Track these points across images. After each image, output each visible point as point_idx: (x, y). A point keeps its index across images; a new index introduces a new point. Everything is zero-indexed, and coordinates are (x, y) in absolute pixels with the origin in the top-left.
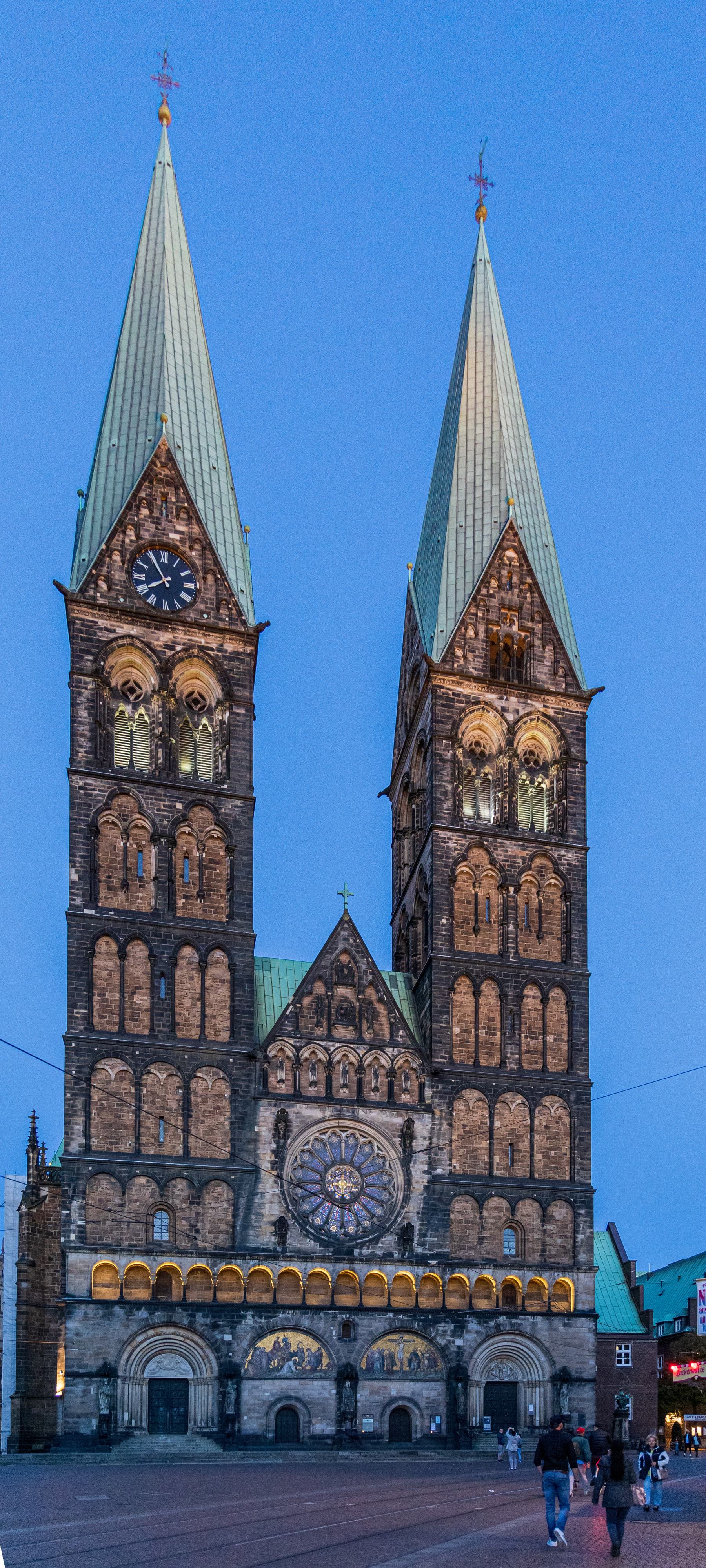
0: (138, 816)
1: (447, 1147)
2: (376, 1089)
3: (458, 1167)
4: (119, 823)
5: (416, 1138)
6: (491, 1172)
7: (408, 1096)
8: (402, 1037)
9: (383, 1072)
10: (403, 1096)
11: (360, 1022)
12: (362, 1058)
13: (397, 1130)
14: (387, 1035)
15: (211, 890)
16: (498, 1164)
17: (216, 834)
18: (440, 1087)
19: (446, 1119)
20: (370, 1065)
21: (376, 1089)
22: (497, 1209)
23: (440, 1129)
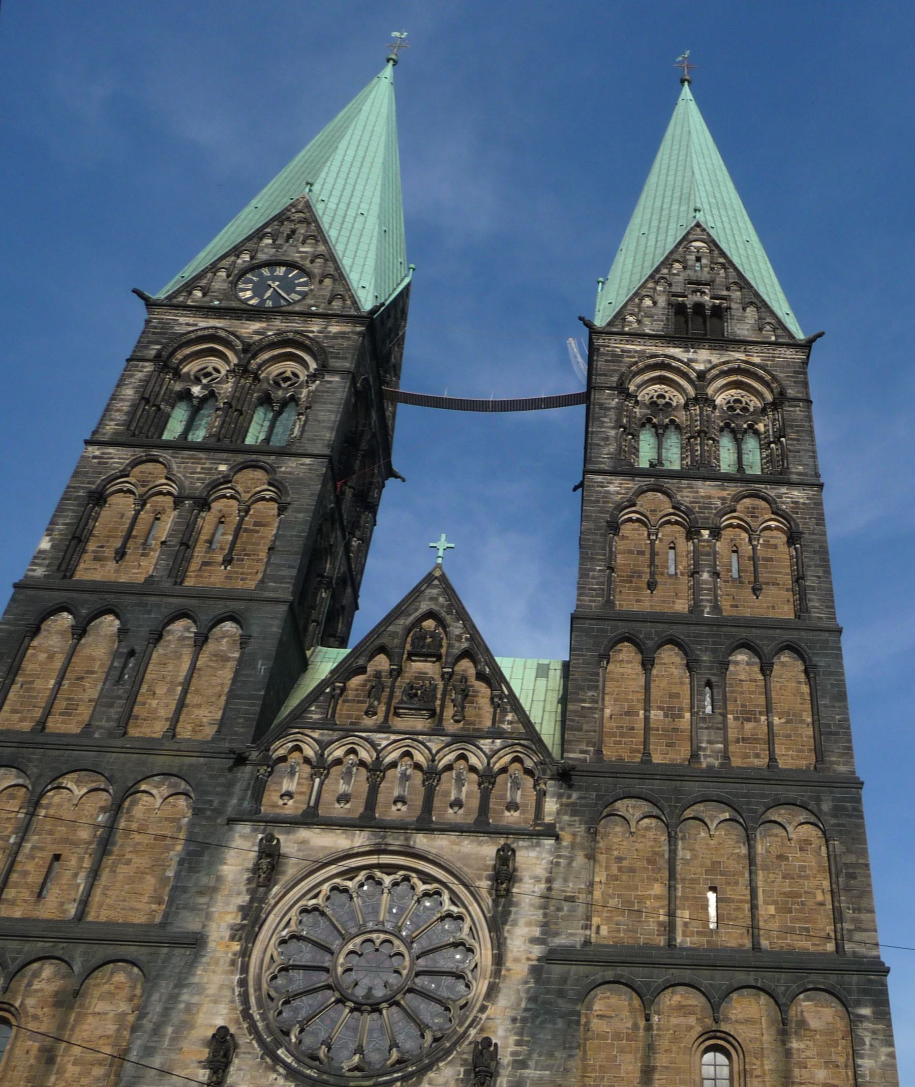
0: (164, 481)
1: (582, 897)
2: (458, 803)
3: (604, 931)
4: (135, 490)
5: (521, 880)
6: (671, 944)
7: (517, 814)
8: (510, 723)
9: (474, 776)
10: (507, 814)
11: (443, 706)
12: (434, 756)
13: (486, 868)
14: (488, 723)
15: (245, 555)
16: (686, 925)
17: (268, 495)
18: (575, 795)
19: (583, 848)
20: (449, 767)
21: (458, 803)
22: (680, 1007)
23: (569, 864)
